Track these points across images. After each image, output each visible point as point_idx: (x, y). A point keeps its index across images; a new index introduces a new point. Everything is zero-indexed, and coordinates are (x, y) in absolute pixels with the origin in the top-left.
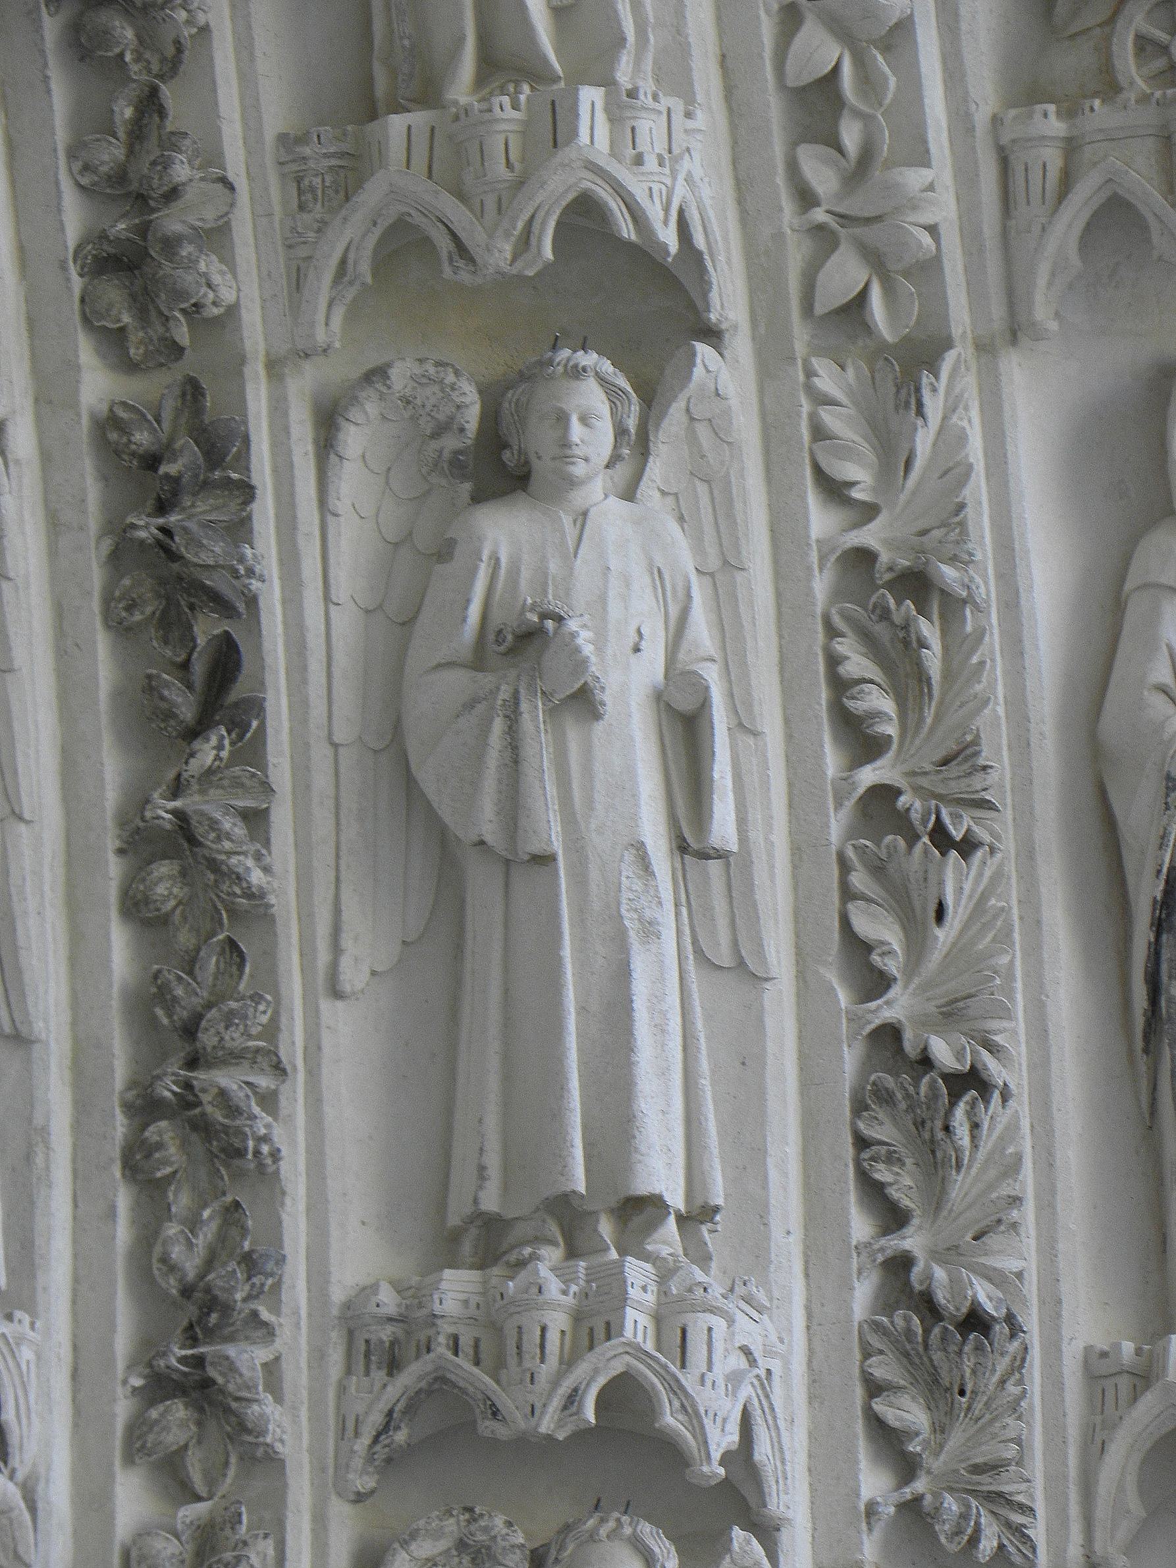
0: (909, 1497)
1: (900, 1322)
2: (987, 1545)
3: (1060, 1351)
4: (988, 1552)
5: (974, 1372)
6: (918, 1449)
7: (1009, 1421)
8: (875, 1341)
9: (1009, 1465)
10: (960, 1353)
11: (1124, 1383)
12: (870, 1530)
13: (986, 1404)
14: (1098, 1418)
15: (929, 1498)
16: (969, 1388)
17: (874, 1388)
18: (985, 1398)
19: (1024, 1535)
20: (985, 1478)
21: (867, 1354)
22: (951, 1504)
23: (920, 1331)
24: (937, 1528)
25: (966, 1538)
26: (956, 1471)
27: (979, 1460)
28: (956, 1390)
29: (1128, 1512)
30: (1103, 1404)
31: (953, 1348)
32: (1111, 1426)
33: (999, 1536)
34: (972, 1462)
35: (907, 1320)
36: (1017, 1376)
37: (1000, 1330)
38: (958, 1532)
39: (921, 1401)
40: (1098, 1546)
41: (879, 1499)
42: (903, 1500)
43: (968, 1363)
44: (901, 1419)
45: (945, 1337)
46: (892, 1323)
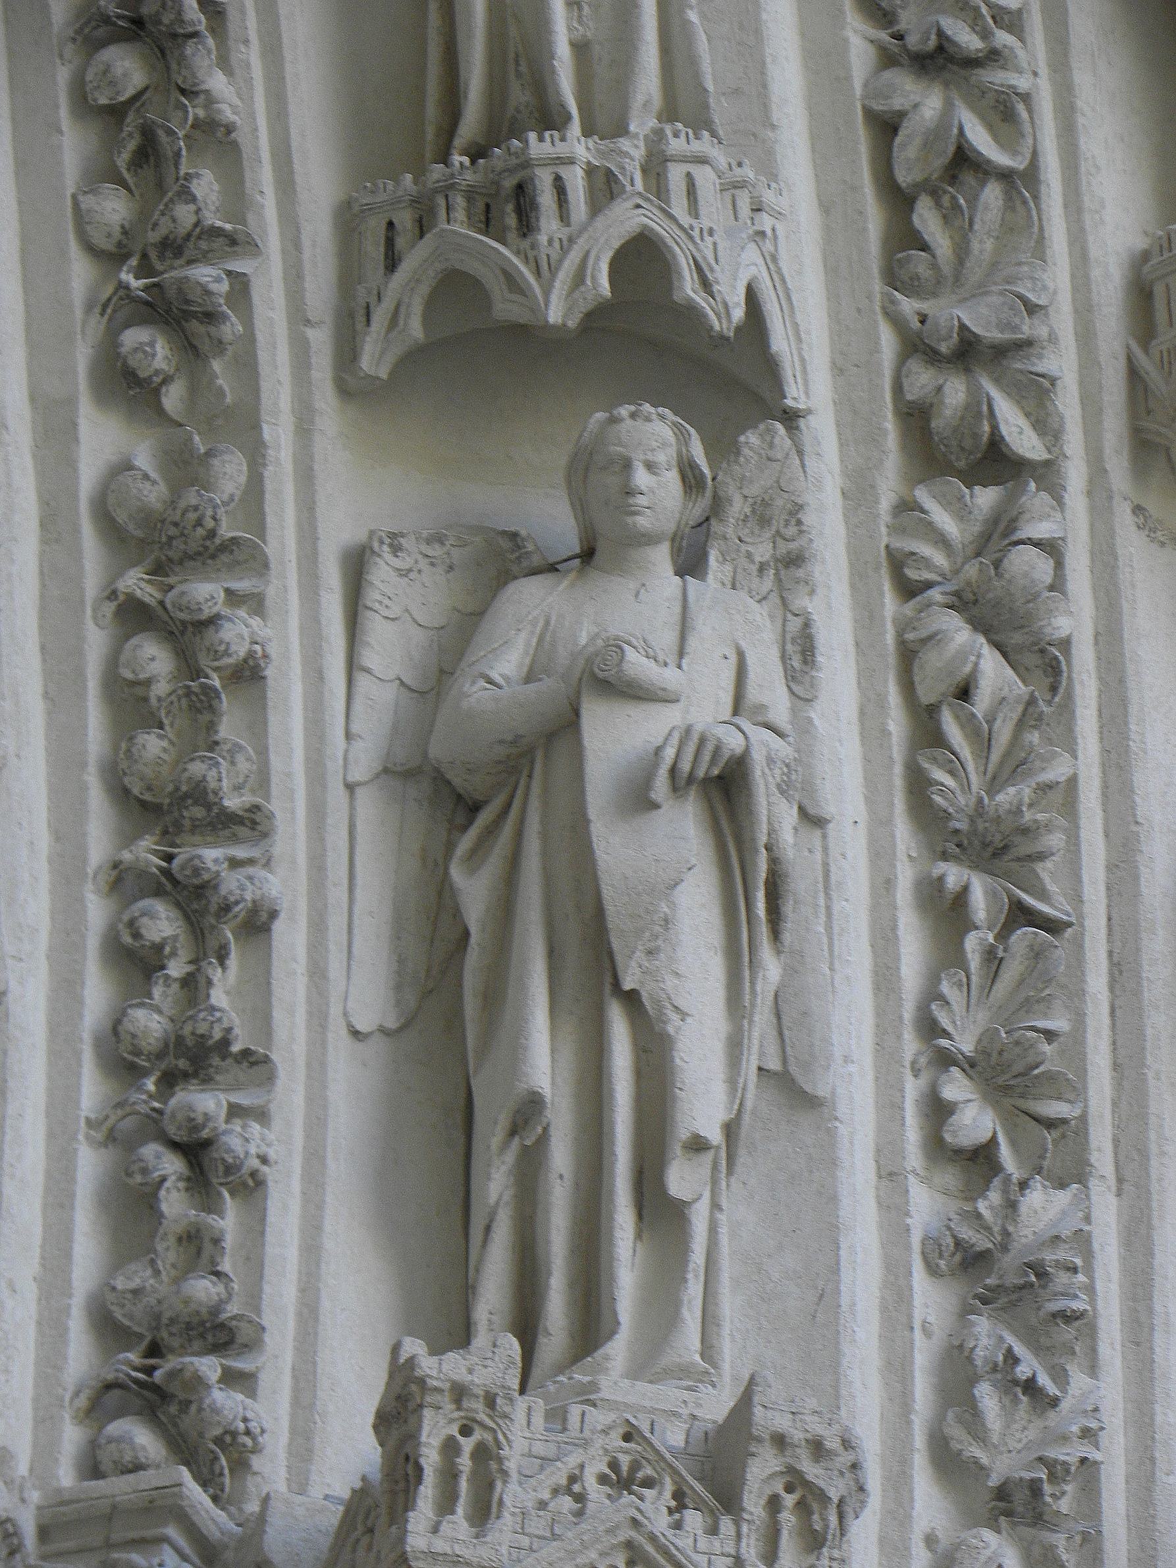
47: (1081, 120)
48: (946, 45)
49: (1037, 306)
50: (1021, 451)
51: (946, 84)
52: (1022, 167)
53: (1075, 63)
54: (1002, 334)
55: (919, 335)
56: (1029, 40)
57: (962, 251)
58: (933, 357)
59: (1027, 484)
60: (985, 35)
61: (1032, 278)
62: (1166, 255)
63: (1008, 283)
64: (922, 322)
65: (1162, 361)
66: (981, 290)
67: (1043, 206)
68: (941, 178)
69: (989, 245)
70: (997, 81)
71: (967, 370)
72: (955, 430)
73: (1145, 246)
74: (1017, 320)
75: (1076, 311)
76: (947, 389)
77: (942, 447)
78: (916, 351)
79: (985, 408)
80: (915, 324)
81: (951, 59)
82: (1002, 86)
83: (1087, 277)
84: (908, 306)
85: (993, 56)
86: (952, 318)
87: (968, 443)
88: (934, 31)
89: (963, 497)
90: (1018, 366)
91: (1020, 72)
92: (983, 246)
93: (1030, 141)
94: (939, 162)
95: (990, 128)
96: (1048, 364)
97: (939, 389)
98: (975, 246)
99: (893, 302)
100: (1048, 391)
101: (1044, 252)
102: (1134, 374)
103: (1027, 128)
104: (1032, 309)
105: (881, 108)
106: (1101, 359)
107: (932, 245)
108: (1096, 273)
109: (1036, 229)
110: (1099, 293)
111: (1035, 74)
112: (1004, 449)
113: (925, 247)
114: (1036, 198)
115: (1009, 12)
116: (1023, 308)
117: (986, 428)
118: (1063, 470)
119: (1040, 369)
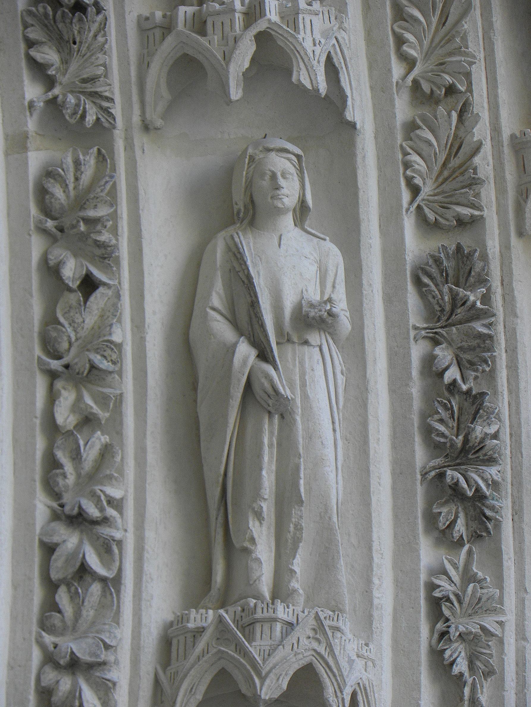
0: (51, 97)
1: (41, 10)
2: (90, 119)
3: (124, 18)
4: (91, 122)
5: (79, 32)
6: (54, 73)
7: (100, 55)
8: (29, 20)
9: (100, 77)
10: (71, 23)
11: (158, 33)
12: (31, 115)
13: (88, 47)
14: (146, 51)
15: (61, 97)
16: (78, 40)
17: (30, 44)
18: (87, 45)
19: (109, 112)
20: (88, 85)
21: (26, 26)
22: (71, 99)
23: (51, 13)
24: (64, 112)
25: (79, 116)
26: (74, 82)
27: (85, 76)
28: (71, 42)
29: (162, 97)
30: (148, 44)
31: (68, 21)
32: (151, 55)
33: (97, 114)
34: (81, 77)
35: (45, 8)
36: (102, 32)
37: (91, 10)
38: (75, 113)
39: (54, 48)
40: (148, 115)
41: (35, 99)
42: (47, 99)
43: (76, 28)
44: (44, 58)
45: (64, 14)
46: (37, 10)
47: (146, 555)
48: (82, 513)
49: (110, 646)
51: (82, 532)
52: (111, 577)
53: (147, 526)
54: (91, 657)
55: (52, 653)
56: (125, 514)
57: (78, 615)
58: (57, 666)
60: (102, 510)
61: (110, 632)
62: (180, 625)
63: (98, 633)
64: (55, 647)
65: (171, 678)
66: (84, 635)
67: (122, 596)
68: (72, 578)
69: (92, 613)
70: (105, 533)
71: (74, 674)
73: (172, 619)
74: (99, 652)
75: (132, 649)
76: (62, 682)
78: (51, 661)
79: (77, 694)
80: (51, 648)
81: (85, 520)
82: (107, 535)
83: (139, 633)
84: (48, 639)
85: (105, 521)
86: (68, 648)
88: (77, 505)
90: (98, 674)
91: (118, 529)
92: (88, 613)
93: (117, 564)
94: (72, 570)
95: (99, 555)
96: (113, 675)
97: (58, 682)
98: (84, 613)
99: (41, 637)
100: (110, 688)
101: (119, 619)
102: (157, 682)
103: (117, 557)
104: (107, 647)
105: (47, 540)
106: (142, 674)
107: (63, 611)
108: (144, 631)
109: (115, 608)
110: (144, 641)
111: (126, 531)
113: (60, 612)
114: (118, 592)
115: (116, 499)
116: (102, 646)
119: (108, 676)
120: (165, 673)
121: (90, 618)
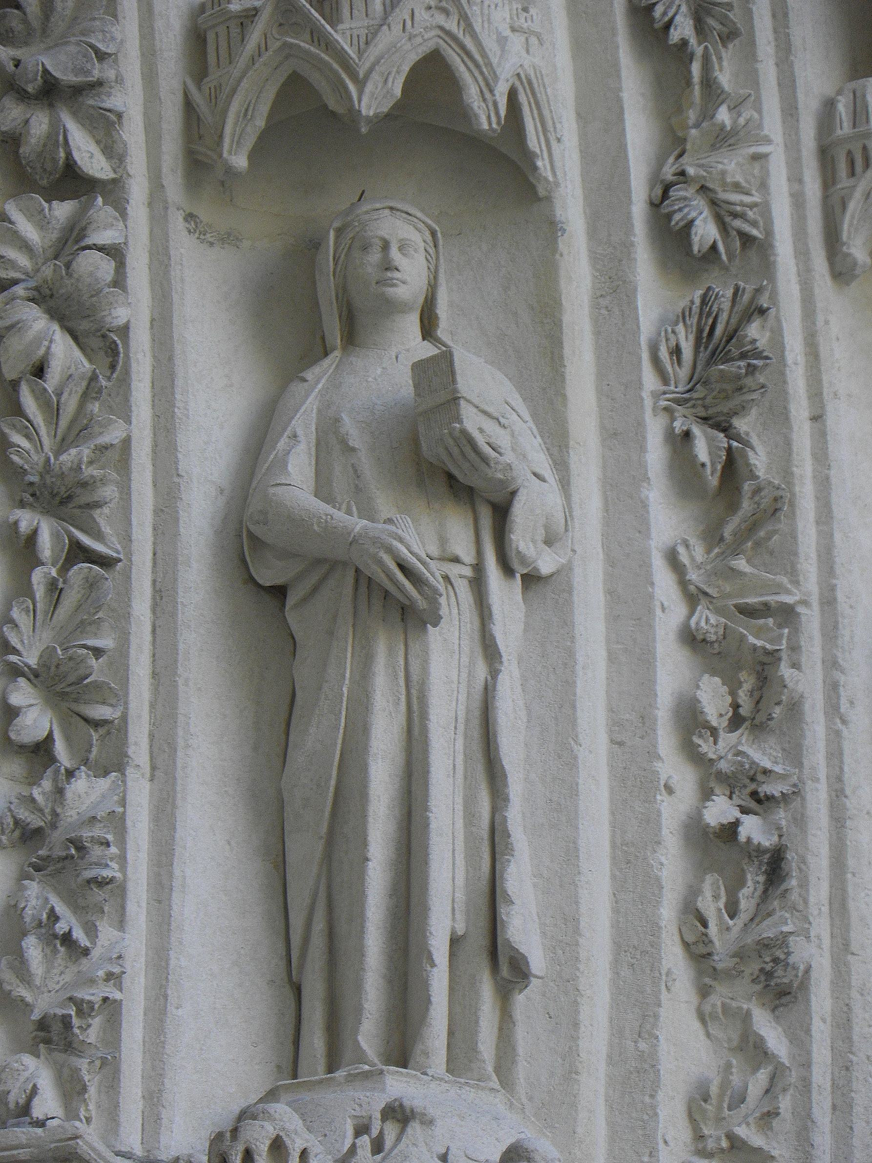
49: (106, 53)
50: (91, 172)
54: (76, 76)
55: (13, 75)
59: (95, 198)
61: (103, 31)
62: (217, 9)
63: (84, 35)
64: (16, 66)
71: (51, 106)
72: (40, 154)
74: (89, 66)
76: (33, 121)
77: (28, 168)
78: (13, 89)
79: (61, 138)
80: (10, 67)
86: (38, 65)
87: (49, 166)
89: (43, 210)
90: (91, 102)
96: (115, 101)
97: (27, 122)
100: (113, 123)
102: (189, 106)
104: (102, 56)
106: (162, 95)
108: (159, 24)
110: (161, 41)
112: (77, 169)
116: (94, 56)
117: (62, 154)
118: (127, 186)
119: (107, 105)
120: (200, 89)
121: (68, 12)
